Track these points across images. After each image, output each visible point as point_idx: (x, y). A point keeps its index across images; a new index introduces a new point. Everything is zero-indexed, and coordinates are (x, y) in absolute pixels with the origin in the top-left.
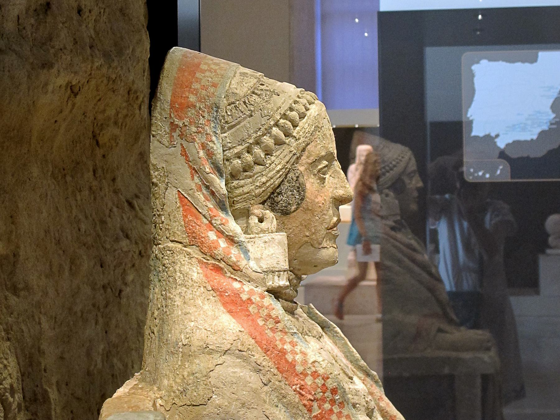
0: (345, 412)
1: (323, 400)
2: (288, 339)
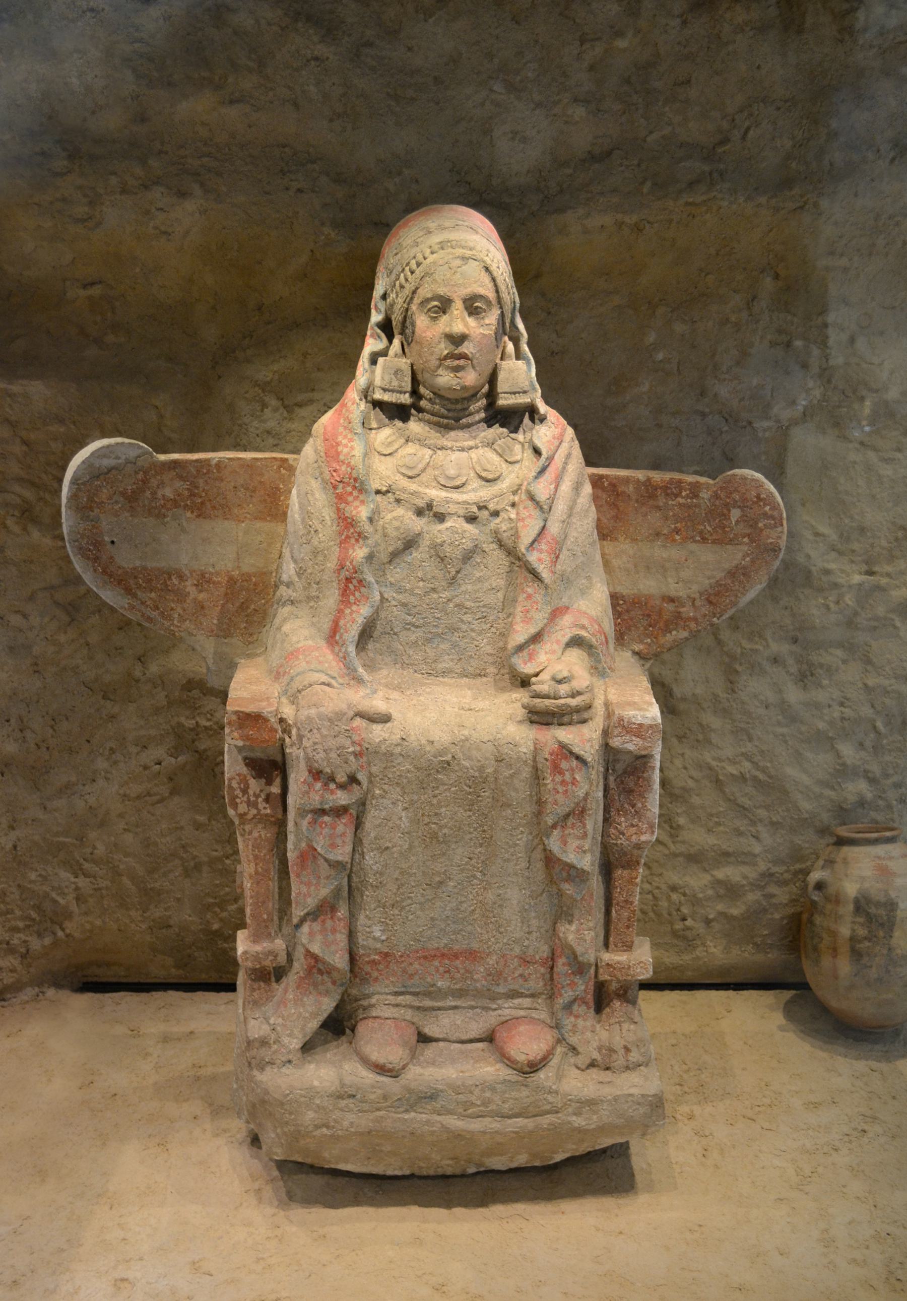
0: (362, 497)
1: (348, 484)
2: (350, 436)
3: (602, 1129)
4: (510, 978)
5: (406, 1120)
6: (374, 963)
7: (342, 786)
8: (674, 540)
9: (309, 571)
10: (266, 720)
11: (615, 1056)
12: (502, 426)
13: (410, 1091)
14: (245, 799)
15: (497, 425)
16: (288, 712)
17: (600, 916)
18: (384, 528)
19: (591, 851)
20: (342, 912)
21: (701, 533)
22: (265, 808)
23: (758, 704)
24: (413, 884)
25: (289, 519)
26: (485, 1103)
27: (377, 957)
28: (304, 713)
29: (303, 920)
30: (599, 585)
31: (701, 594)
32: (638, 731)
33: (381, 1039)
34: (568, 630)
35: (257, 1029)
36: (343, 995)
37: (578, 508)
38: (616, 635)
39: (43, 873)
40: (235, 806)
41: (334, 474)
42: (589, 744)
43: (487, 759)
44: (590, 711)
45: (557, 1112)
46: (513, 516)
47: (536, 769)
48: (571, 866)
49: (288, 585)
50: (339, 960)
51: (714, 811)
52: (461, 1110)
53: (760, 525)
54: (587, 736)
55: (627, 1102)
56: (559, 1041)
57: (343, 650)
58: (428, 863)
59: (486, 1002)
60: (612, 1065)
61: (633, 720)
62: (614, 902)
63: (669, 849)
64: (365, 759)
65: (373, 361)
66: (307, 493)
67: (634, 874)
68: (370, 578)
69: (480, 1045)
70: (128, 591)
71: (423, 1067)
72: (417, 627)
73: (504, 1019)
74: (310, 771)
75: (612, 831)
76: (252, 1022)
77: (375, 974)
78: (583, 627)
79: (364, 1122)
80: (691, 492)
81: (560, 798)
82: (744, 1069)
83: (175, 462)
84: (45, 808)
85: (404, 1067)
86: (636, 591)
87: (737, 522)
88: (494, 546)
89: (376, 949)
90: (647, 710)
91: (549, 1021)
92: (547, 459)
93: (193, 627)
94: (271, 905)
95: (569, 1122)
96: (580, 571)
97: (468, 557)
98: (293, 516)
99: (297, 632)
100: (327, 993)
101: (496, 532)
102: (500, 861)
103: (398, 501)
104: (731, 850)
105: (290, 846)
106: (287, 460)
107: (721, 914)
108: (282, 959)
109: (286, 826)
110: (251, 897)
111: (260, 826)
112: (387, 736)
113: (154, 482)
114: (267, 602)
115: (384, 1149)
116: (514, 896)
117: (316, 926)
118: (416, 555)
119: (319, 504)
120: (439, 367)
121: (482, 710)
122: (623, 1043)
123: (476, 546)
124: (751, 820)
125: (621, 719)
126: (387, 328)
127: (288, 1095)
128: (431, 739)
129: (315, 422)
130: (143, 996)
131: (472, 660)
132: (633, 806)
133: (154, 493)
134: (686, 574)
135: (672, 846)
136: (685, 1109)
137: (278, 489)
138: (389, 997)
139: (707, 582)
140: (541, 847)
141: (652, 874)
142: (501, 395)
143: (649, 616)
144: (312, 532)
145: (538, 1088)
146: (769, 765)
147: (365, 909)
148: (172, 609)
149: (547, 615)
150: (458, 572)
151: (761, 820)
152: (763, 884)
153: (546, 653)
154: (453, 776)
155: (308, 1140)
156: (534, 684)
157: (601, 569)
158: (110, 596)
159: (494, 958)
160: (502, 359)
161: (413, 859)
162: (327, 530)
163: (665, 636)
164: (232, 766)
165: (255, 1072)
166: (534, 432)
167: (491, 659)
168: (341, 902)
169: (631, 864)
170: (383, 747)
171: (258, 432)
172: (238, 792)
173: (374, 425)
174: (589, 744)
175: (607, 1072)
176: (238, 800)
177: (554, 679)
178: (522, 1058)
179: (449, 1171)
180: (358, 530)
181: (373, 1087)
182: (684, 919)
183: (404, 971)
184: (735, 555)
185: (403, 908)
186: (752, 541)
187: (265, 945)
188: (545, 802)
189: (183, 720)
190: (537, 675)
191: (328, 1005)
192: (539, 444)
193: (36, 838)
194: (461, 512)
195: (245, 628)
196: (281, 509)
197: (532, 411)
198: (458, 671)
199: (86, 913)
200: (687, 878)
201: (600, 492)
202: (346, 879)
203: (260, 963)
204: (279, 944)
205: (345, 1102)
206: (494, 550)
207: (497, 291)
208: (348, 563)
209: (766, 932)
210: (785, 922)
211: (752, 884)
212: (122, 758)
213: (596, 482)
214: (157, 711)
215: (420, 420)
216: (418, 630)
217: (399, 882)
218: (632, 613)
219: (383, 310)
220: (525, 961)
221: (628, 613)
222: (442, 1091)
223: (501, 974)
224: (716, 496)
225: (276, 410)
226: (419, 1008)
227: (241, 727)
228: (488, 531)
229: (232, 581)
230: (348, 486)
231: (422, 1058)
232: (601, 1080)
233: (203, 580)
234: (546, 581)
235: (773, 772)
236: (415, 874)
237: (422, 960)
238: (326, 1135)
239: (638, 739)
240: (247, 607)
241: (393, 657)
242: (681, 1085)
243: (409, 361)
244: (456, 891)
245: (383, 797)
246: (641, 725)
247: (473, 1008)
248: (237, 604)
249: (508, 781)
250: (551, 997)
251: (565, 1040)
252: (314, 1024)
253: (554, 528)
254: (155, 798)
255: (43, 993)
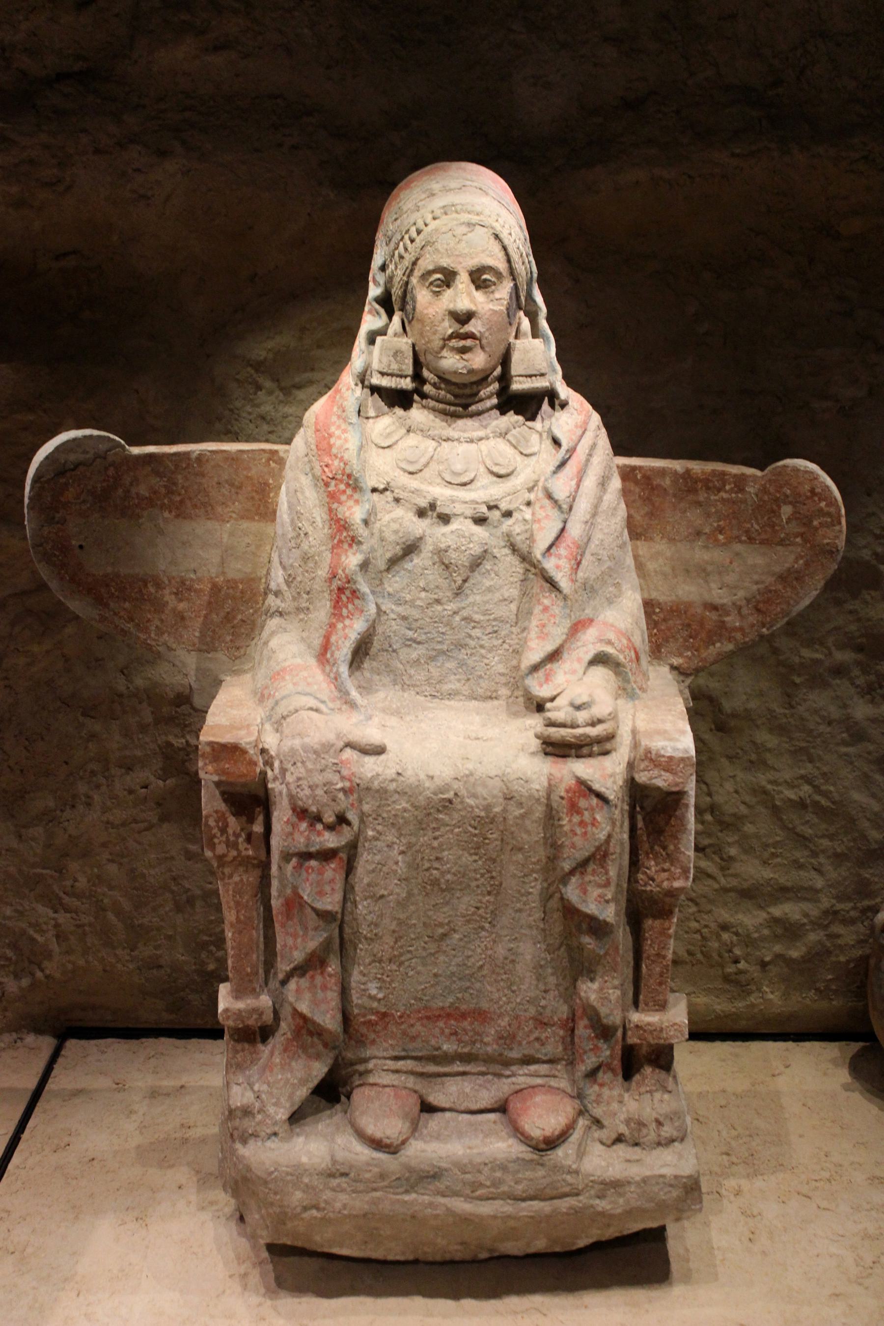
0: (356, 496)
1: (341, 481)
2: (343, 426)
3: (629, 1213)
4: (524, 1042)
5: (406, 1202)
7: (330, 828)
8: (717, 540)
9: (299, 579)
10: (244, 752)
11: (645, 1131)
12: (517, 413)
13: (410, 1169)
14: (224, 838)
15: (512, 412)
16: (271, 741)
17: (629, 972)
18: (381, 531)
19: (615, 899)
20: (333, 967)
21: (747, 532)
22: (246, 849)
23: (819, 721)
24: (413, 936)
25: (278, 520)
26: (496, 1184)
27: (373, 1017)
28: (288, 744)
29: (289, 976)
30: (630, 592)
31: (748, 601)
32: (668, 764)
33: (380, 1107)
34: (591, 646)
35: (240, 1096)
36: (336, 1059)
37: (604, 506)
38: (651, 647)
39: (20, 908)
40: (212, 847)
41: (326, 469)
42: (612, 779)
43: (494, 797)
44: (613, 741)
45: (577, 1195)
46: (528, 516)
47: (549, 807)
48: (592, 918)
49: (277, 594)
51: (771, 841)
52: (468, 1192)
53: (815, 523)
54: (609, 770)
55: (657, 1183)
56: (581, 1113)
57: (335, 670)
58: (430, 913)
59: (497, 1068)
60: (642, 1140)
61: (662, 752)
62: (645, 955)
63: (718, 883)
64: (356, 795)
65: (371, 341)
66: (296, 491)
67: (667, 924)
68: (364, 587)
69: (492, 1116)
70: (100, 601)
71: (425, 1142)
72: (419, 643)
73: (518, 1087)
74: (294, 810)
75: (640, 876)
76: (235, 1089)
78: (609, 642)
79: (359, 1203)
80: (736, 486)
81: (578, 841)
82: (801, 1136)
83: (151, 456)
84: (20, 836)
85: (404, 1142)
86: (674, 598)
87: (789, 520)
88: (507, 551)
89: (372, 1009)
90: (677, 740)
91: (569, 1090)
92: (567, 451)
93: (172, 640)
94: (254, 956)
95: (592, 1206)
96: (606, 577)
97: (476, 564)
98: (281, 517)
99: (286, 647)
100: (318, 1057)
101: (508, 535)
102: (511, 911)
103: (397, 500)
104: (789, 884)
105: (274, 892)
106: (276, 452)
107: (778, 956)
108: (268, 1017)
109: (270, 869)
110: (233, 948)
111: (241, 869)
112: (380, 770)
114: (256, 612)
115: (382, 1232)
116: (526, 949)
117: (304, 982)
118: (417, 562)
119: (310, 503)
120: (442, 348)
121: (491, 739)
122: (654, 1115)
123: (485, 551)
124: (812, 851)
125: (648, 751)
126: (386, 302)
127: (272, 1172)
128: (431, 774)
129: (306, 410)
130: (134, 1044)
131: (481, 681)
132: (665, 848)
134: (730, 579)
135: (723, 881)
136: (731, 1183)
137: (267, 484)
138: (389, 1062)
139: (755, 587)
140: (557, 895)
141: (699, 911)
142: (515, 379)
143: (689, 625)
144: (300, 534)
145: (557, 1168)
146: (832, 788)
147: (359, 965)
148: (149, 621)
149: (566, 630)
150: (465, 581)
151: (823, 851)
152: (826, 923)
153: (565, 673)
154: (456, 816)
155: (296, 1223)
156: (549, 710)
157: (634, 574)
158: (75, 605)
159: (507, 1019)
160: (516, 337)
161: (412, 908)
162: (318, 534)
163: (707, 648)
164: (210, 802)
165: (238, 1146)
166: (553, 420)
167: (503, 680)
168: (332, 956)
169: (665, 913)
170: (376, 783)
171: (251, 417)
173: (372, 413)
174: (612, 779)
175: (637, 1149)
176: (216, 841)
177: (572, 705)
178: (536, 1133)
179: (458, 1257)
180: (351, 533)
181: (368, 1164)
182: (736, 961)
183: (404, 1033)
185: (401, 964)
186: (806, 541)
187: (249, 1001)
188: (562, 846)
189: (171, 738)
190: (552, 699)
191: (319, 1070)
192: (559, 434)
193: (12, 869)
194: (469, 513)
195: (231, 641)
196: (270, 506)
197: (551, 395)
198: (466, 693)
199: (67, 952)
200: (740, 916)
201: (631, 486)
202: (337, 931)
203: (243, 1022)
204: (265, 1001)
205: (337, 1181)
206: (506, 555)
207: (509, 261)
208: (340, 572)
209: (830, 977)
210: (852, 965)
211: (812, 922)
212: (104, 781)
213: (627, 474)
214: (143, 728)
215: (424, 407)
216: (420, 646)
217: (396, 935)
218: (671, 622)
219: (382, 282)
220: (541, 1023)
221: (664, 624)
222: (446, 1170)
223: (514, 1037)
224: (764, 490)
225: (270, 393)
226: (422, 1075)
228: (499, 534)
229: (216, 589)
230: (341, 483)
231: (425, 1132)
232: (628, 1157)
233: (183, 589)
234: (565, 591)
235: (837, 797)
236: (415, 925)
237: (425, 1021)
238: (315, 1218)
239: (668, 774)
240: (233, 618)
241: (392, 676)
242: (728, 1154)
243: (410, 341)
244: (462, 944)
245: (377, 839)
246: (671, 758)
247: (483, 1074)
248: (222, 614)
249: (519, 821)
250: (571, 1063)
251: (587, 1111)
252: (303, 1092)
253: (575, 530)
254: (142, 826)
255: (21, 1039)
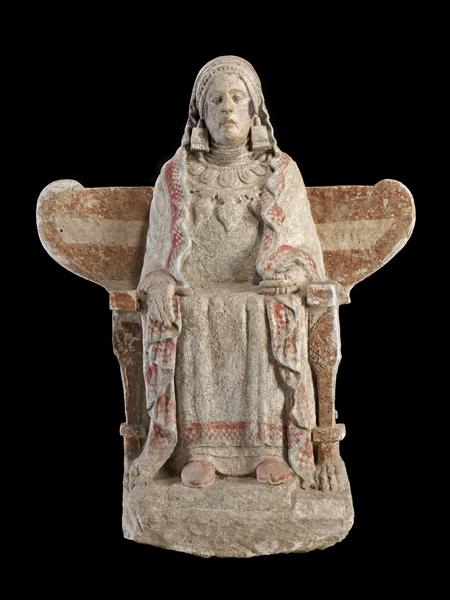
6: (190, 429)
10: (130, 297)
21: (369, 214)
50: (173, 428)
70: (69, 255)
77: (191, 437)
113: (82, 201)
133: (82, 205)
172: (118, 340)
184: (388, 224)
227: (117, 300)
246: (321, 291)
